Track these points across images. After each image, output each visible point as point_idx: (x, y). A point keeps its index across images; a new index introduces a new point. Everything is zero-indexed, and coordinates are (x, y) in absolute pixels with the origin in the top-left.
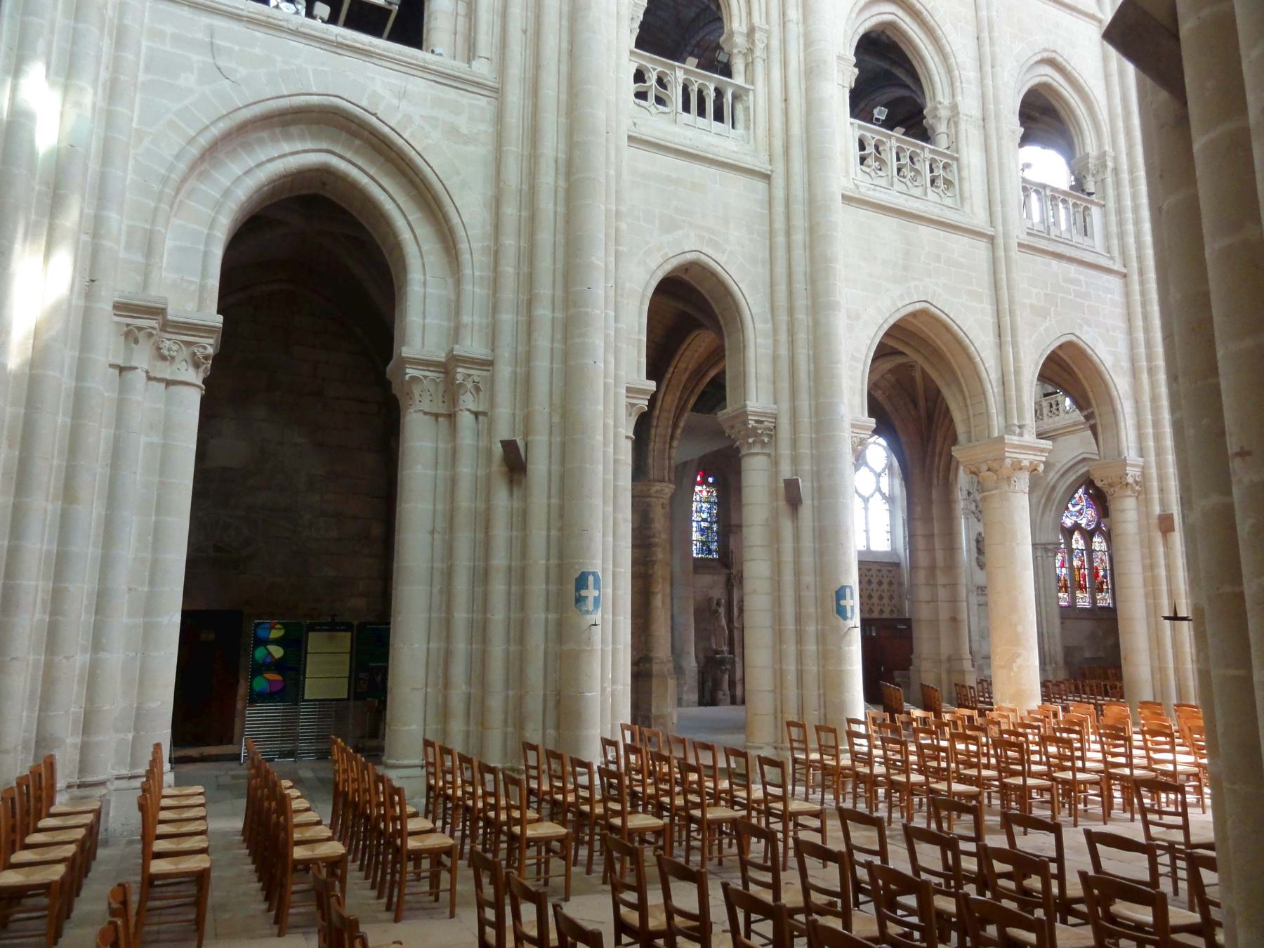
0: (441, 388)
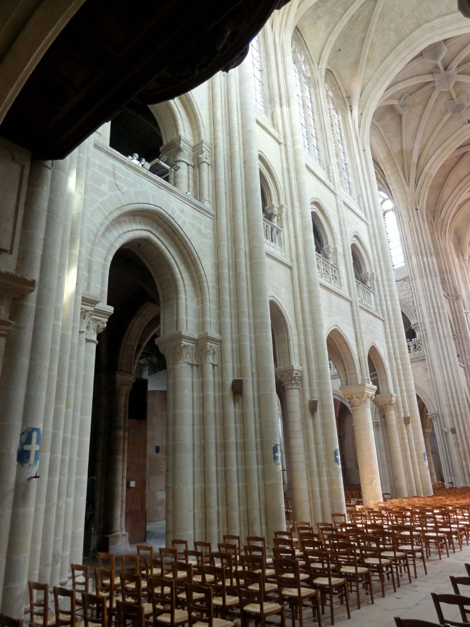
0: (194, 351)
